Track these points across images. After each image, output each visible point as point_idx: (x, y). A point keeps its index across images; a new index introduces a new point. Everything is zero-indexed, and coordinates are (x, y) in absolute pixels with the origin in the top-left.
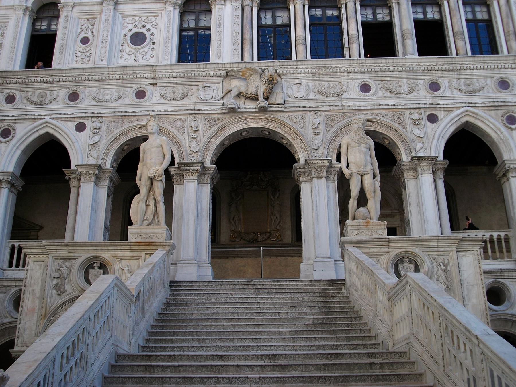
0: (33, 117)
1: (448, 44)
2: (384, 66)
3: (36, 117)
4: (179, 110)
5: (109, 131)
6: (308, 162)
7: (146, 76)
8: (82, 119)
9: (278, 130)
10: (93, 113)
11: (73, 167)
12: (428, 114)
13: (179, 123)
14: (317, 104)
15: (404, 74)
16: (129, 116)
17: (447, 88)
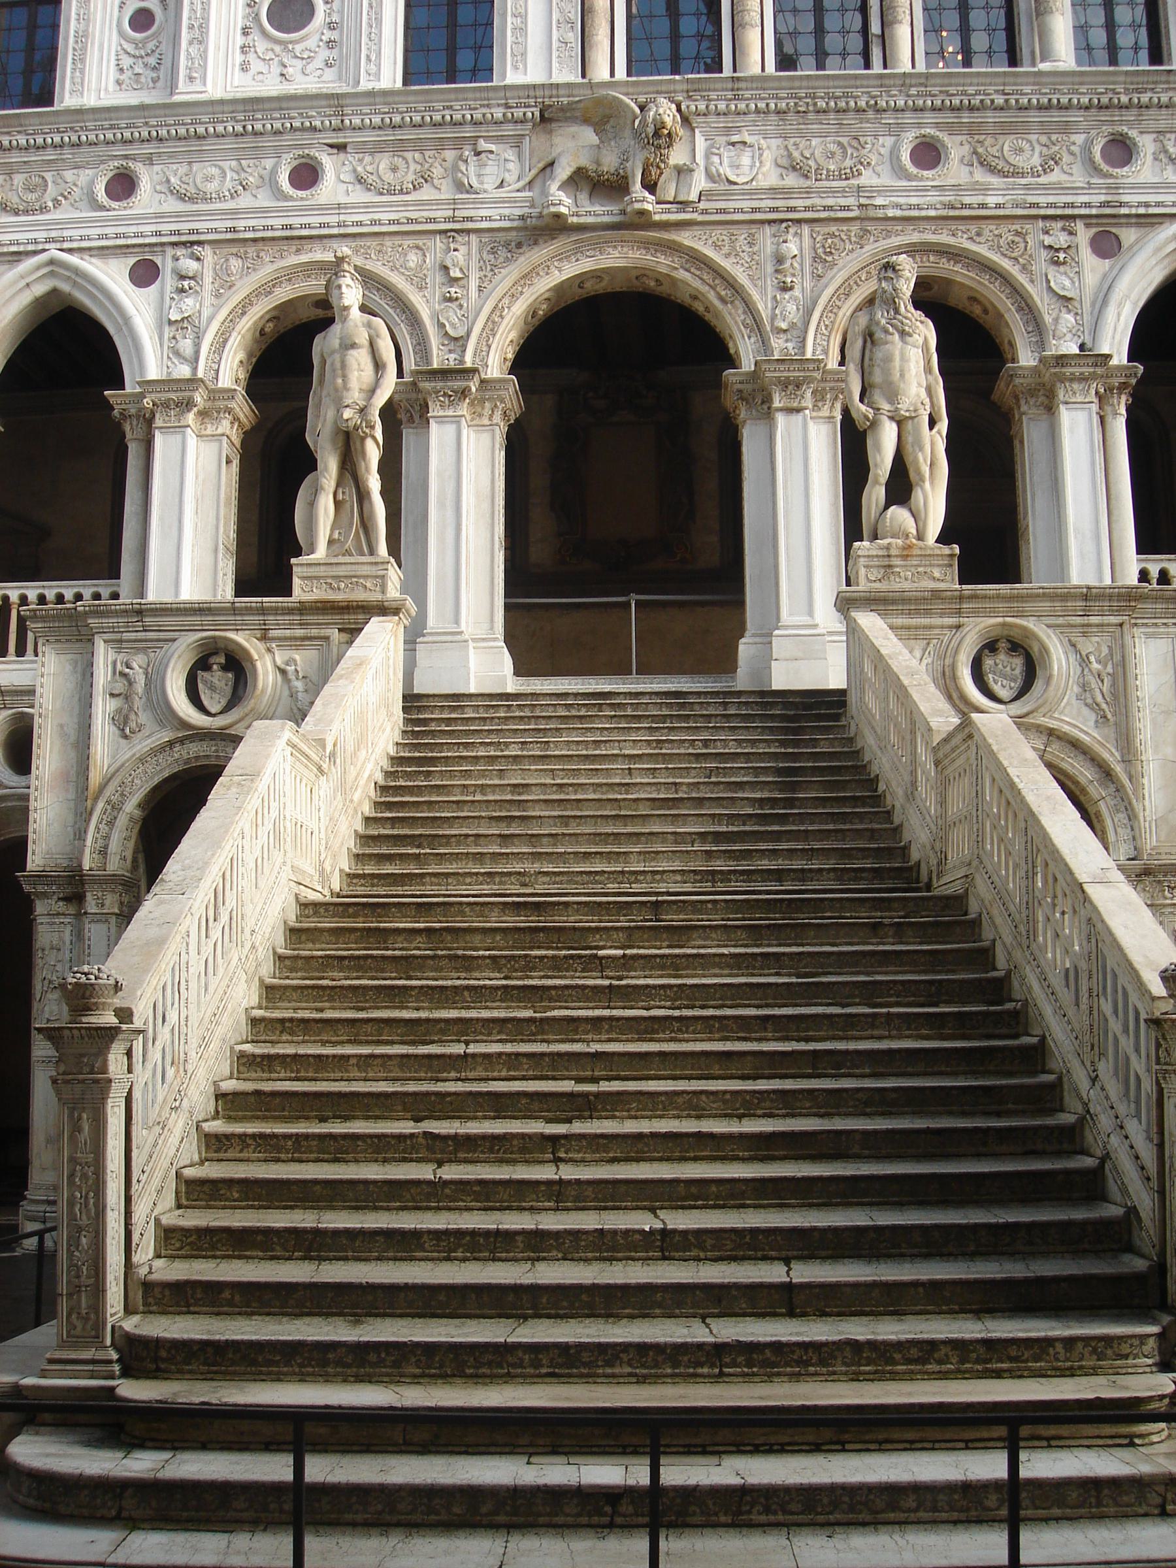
0: (14, 249)
1: (1163, 25)
2: (978, 93)
3: (21, 248)
4: (410, 221)
5: (225, 284)
6: (764, 366)
7: (317, 123)
8: (147, 249)
9: (682, 274)
10: (178, 233)
11: (130, 388)
12: (1094, 230)
13: (413, 259)
14: (792, 203)
15: (1034, 117)
16: (273, 239)
17: (1150, 158)
